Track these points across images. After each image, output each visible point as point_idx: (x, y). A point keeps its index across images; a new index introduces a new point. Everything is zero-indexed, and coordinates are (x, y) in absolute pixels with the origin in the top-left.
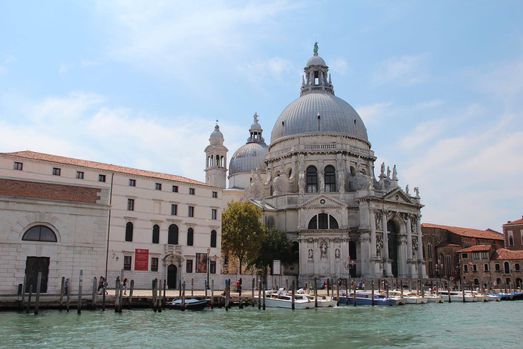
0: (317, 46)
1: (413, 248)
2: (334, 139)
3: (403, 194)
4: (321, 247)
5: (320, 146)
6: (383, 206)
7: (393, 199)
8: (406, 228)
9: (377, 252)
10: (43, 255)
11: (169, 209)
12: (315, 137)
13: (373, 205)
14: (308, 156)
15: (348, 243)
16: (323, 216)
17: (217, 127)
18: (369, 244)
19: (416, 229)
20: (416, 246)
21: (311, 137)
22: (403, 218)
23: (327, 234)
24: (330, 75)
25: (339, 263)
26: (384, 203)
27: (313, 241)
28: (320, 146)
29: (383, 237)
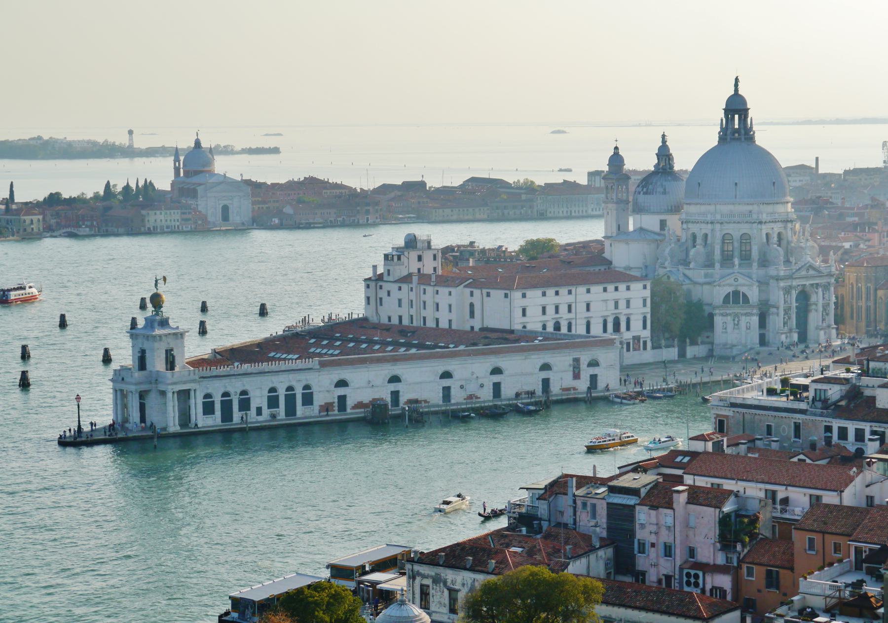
1: (824, 314)
2: (750, 208)
4: (734, 320)
6: (792, 282)
7: (804, 273)
9: (784, 324)
10: (596, 373)
11: (612, 305)
13: (782, 284)
15: (758, 318)
16: (736, 293)
17: (616, 148)
18: (777, 318)
23: (740, 308)
24: (751, 119)
26: (793, 279)
27: (727, 315)
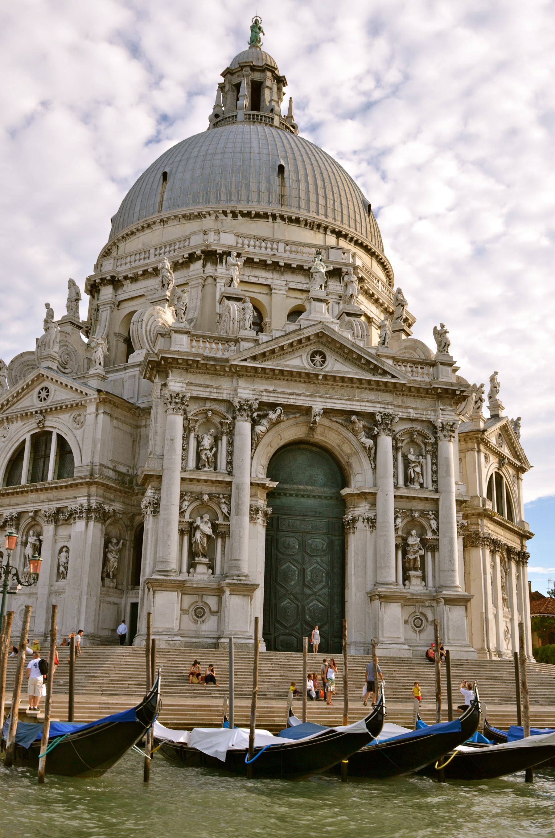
0: (260, 28)
1: (413, 540)
3: (342, 346)
4: (25, 544)
5: (152, 251)
8: (374, 469)
12: (147, 231)
14: (125, 288)
19: (435, 472)
20: (429, 535)
21: (139, 234)
22: (355, 433)
23: (43, 496)
25: (63, 596)
26: (240, 376)
28: (152, 251)
29: (229, 498)
